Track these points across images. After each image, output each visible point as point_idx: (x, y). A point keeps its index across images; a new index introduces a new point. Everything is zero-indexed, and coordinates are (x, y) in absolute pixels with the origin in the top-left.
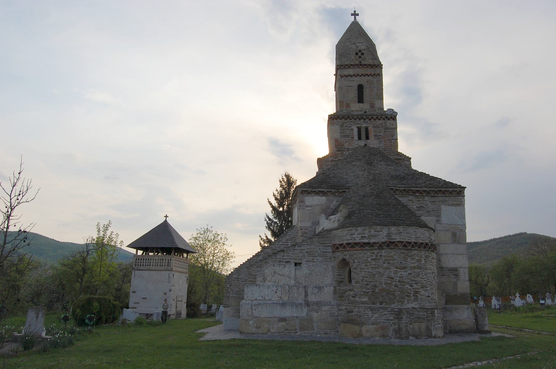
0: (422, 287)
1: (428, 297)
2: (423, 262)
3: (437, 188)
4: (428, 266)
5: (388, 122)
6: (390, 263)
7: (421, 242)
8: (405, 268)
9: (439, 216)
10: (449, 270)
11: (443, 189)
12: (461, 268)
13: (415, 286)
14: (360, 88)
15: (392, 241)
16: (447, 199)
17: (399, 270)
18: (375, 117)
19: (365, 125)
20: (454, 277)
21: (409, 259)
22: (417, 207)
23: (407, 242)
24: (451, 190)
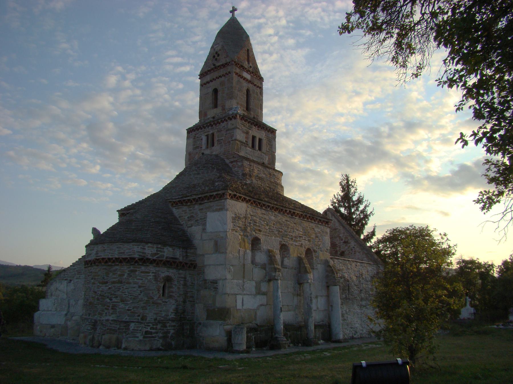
0: (122, 301)
1: (128, 310)
2: (125, 276)
3: (202, 194)
4: (131, 281)
5: (230, 122)
6: (95, 279)
7: (124, 257)
8: (107, 283)
9: (205, 224)
10: (211, 282)
11: (208, 195)
12: (220, 279)
13: (114, 300)
14: (216, 91)
15: (98, 258)
16: (211, 204)
17: (101, 285)
18: (219, 121)
19: (211, 132)
20: (213, 290)
21: (111, 274)
22: (188, 218)
23: (109, 259)
24: (215, 193)
